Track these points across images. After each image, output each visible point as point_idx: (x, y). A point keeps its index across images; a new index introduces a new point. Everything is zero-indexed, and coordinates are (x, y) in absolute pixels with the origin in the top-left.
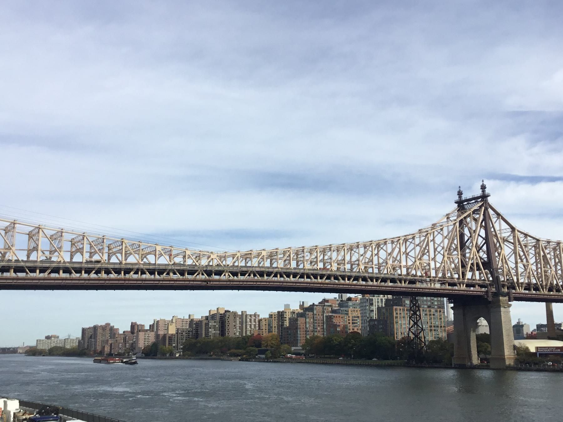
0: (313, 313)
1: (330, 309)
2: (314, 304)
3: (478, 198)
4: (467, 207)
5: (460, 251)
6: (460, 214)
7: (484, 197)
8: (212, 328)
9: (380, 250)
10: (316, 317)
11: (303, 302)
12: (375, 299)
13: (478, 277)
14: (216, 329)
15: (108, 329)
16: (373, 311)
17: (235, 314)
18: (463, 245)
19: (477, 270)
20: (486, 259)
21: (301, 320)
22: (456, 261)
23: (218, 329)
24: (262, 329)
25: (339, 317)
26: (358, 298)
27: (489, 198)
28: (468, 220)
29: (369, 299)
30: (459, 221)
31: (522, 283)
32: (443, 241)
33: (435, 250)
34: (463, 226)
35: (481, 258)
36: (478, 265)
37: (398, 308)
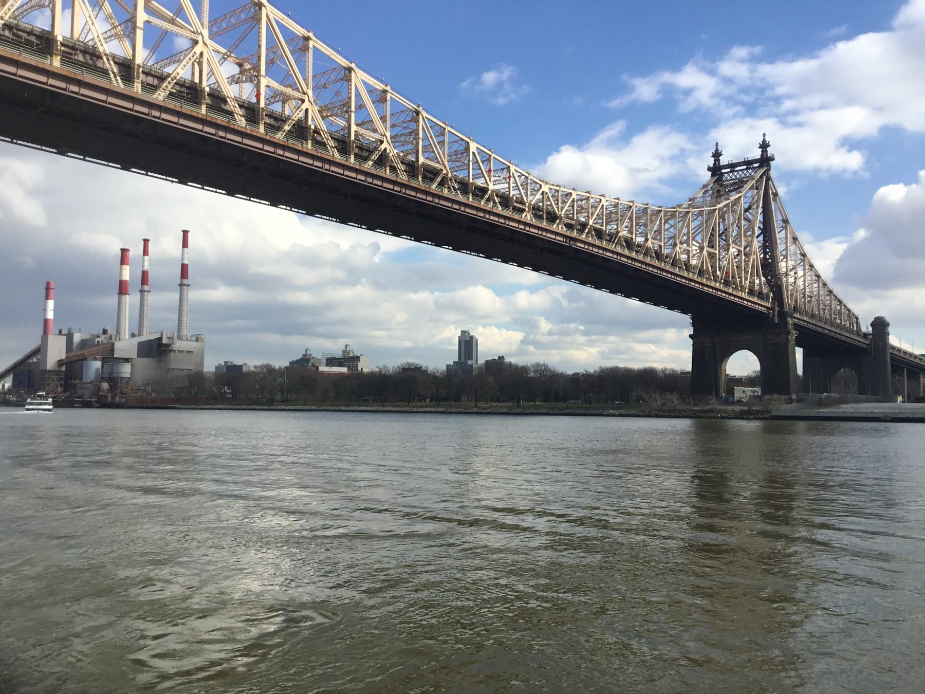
3: (755, 161)
7: (765, 161)
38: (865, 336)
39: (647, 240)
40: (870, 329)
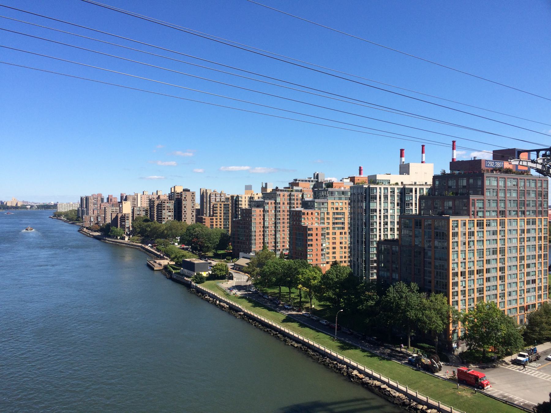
0: (276, 201)
1: (300, 196)
2: (277, 188)
8: (166, 209)
10: (280, 207)
11: (266, 184)
12: (380, 188)
14: (171, 210)
15: (99, 198)
16: (376, 210)
17: (193, 193)
21: (257, 212)
23: (173, 210)
24: (217, 216)
25: (312, 213)
26: (343, 184)
29: (369, 188)
37: (460, 219)
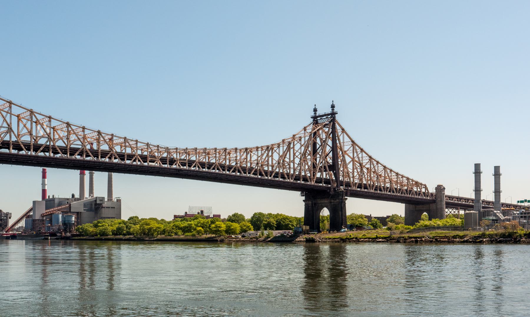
3: (328, 115)
4: (320, 121)
5: (313, 156)
6: (314, 127)
7: (333, 114)
9: (274, 152)
13: (324, 177)
18: (315, 151)
19: (324, 171)
20: (331, 164)
22: (309, 164)
27: (336, 115)
28: (321, 131)
30: (314, 133)
31: (356, 183)
32: (300, 148)
33: (294, 154)
34: (316, 137)
35: (328, 162)
36: (325, 167)
38: (432, 194)
39: (236, 164)
40: (435, 191)
